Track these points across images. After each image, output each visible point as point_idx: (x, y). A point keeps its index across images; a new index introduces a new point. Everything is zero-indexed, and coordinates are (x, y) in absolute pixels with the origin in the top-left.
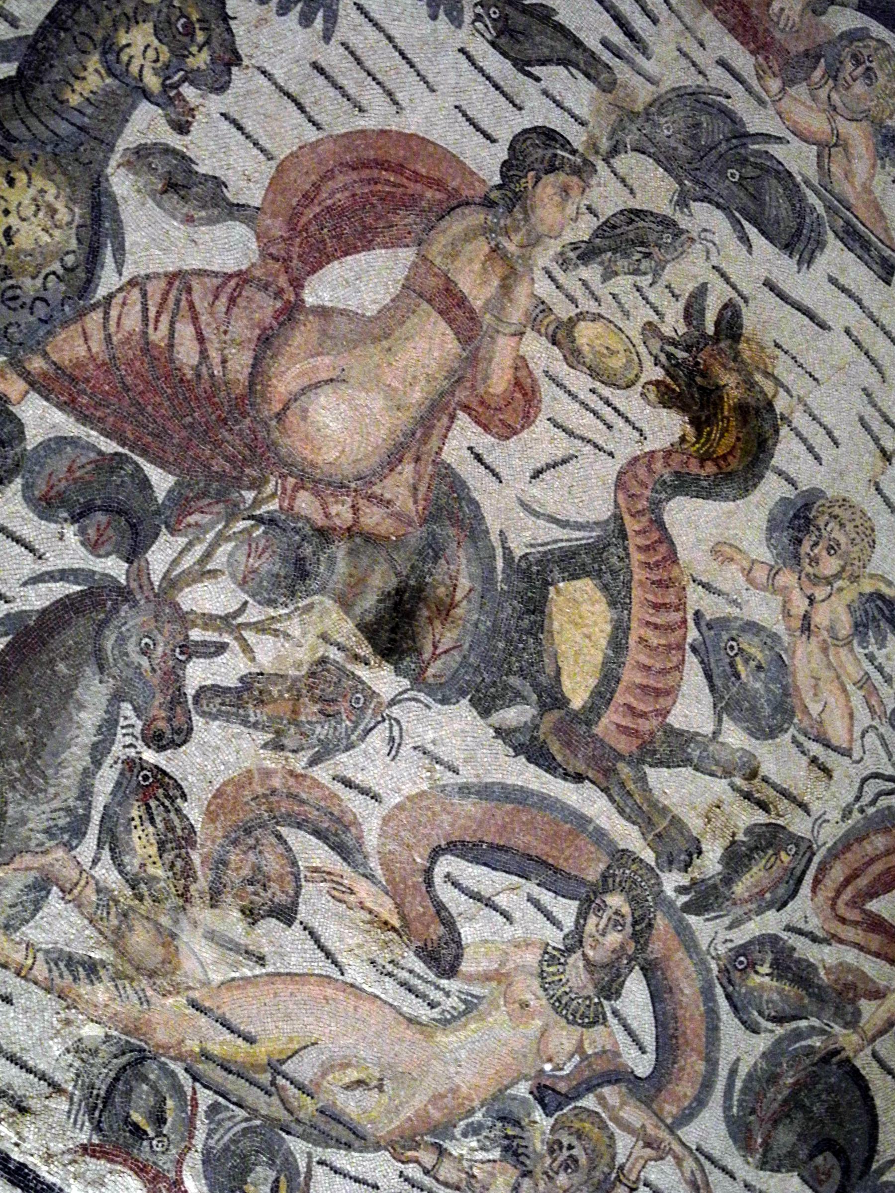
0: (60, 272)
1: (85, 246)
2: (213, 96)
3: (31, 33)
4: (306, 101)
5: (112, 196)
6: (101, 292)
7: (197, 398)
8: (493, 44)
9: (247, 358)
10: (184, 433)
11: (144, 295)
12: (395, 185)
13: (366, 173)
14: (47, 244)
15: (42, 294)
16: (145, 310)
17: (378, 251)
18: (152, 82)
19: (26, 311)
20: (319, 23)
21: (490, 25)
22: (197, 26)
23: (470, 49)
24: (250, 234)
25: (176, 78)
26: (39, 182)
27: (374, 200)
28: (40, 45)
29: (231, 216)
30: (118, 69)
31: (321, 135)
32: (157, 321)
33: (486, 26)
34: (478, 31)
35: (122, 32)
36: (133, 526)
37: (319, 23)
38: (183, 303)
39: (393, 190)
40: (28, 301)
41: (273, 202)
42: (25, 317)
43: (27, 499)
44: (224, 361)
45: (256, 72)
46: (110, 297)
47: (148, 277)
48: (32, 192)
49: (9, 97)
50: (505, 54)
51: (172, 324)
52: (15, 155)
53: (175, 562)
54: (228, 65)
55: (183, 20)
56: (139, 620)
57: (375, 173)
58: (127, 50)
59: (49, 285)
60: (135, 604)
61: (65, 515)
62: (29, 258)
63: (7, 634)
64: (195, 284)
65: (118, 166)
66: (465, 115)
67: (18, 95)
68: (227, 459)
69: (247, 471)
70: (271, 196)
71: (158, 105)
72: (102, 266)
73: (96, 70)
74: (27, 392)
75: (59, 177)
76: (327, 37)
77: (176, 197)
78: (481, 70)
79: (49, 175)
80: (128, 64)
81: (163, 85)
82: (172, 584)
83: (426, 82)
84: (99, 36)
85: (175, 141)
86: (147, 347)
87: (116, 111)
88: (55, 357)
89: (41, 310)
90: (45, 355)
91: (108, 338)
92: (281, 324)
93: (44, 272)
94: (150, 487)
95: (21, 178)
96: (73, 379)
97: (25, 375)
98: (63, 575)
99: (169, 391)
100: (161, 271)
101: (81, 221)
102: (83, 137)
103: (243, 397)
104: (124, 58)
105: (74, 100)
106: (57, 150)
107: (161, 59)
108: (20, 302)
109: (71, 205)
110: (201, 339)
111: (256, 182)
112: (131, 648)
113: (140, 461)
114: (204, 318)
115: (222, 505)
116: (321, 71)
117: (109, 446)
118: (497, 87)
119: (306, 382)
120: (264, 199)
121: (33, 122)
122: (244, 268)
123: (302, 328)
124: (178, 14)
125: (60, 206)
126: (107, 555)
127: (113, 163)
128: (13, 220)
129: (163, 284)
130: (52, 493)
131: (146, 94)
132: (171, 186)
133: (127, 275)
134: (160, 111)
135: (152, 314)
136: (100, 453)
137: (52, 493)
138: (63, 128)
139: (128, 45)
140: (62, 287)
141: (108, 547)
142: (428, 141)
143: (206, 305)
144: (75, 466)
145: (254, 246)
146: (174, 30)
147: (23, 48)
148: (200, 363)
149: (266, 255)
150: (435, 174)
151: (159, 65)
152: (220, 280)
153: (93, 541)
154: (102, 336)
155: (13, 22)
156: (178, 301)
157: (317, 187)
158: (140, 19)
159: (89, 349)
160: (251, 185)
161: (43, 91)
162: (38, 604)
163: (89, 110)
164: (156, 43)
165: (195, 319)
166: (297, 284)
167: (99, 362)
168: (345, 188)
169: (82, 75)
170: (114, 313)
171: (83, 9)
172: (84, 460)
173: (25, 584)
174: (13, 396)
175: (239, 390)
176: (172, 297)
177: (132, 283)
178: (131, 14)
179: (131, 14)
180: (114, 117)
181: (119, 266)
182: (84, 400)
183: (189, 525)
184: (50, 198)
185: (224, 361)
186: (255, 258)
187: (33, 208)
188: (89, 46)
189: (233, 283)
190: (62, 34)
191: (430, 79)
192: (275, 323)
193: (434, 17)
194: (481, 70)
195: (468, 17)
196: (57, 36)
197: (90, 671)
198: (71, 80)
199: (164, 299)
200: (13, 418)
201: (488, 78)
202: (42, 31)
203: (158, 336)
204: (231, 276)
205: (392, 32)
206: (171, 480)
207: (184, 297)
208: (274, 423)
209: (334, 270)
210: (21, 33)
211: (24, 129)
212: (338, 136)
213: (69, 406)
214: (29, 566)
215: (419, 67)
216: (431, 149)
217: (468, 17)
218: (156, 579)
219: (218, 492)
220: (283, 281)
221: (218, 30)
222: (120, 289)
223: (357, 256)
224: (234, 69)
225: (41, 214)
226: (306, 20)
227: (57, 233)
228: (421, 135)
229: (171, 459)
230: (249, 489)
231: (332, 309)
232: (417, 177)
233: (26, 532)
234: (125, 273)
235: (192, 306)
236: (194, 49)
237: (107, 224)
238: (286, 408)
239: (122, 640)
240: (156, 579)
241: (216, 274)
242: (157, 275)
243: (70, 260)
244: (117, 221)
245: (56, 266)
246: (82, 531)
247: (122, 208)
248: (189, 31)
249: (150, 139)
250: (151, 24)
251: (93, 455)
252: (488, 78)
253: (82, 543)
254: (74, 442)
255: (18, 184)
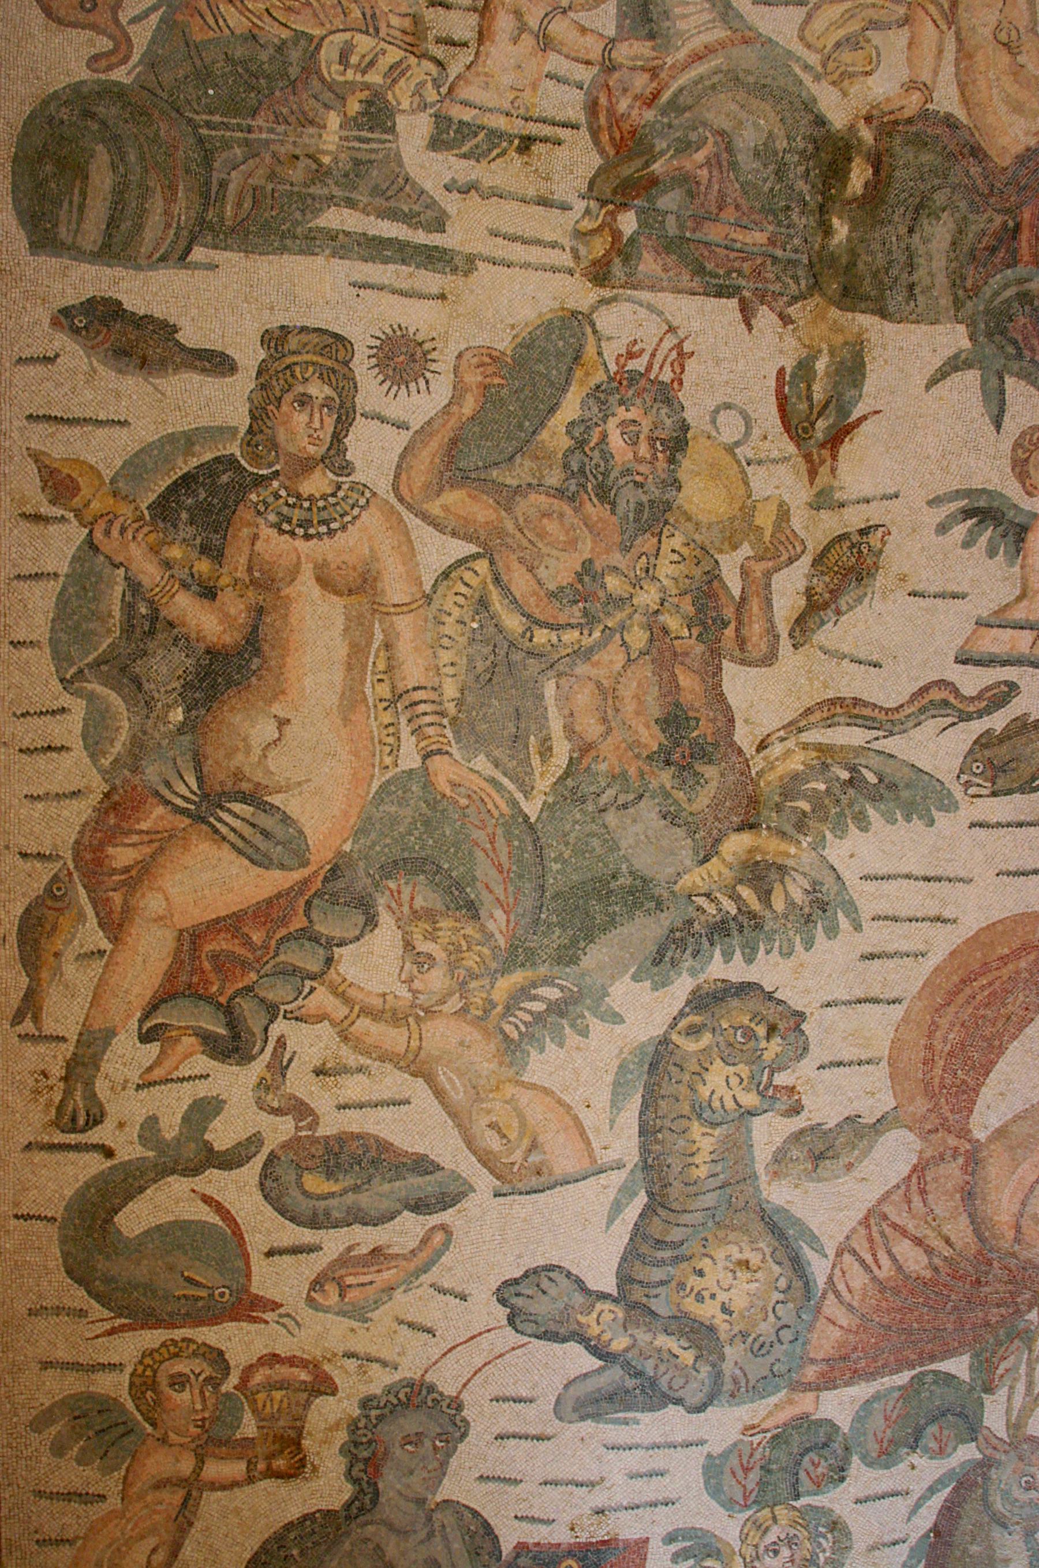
0: (781, 1297)
1: (787, 1262)
2: (802, 1062)
3: (637, 1159)
4: (875, 992)
5: (780, 1210)
6: (821, 1281)
7: (945, 1286)
8: (994, 794)
9: (964, 1220)
10: (952, 1318)
11: (854, 1252)
12: (990, 984)
13: (960, 999)
14: (758, 1289)
15: (780, 1324)
16: (862, 1262)
17: (1011, 1047)
18: (749, 1099)
19: (777, 1345)
20: (844, 922)
21: (981, 782)
22: (753, 1025)
23: (980, 817)
24: (904, 1132)
25: (765, 1078)
26: (720, 1254)
27: (982, 1012)
28: (650, 1161)
29: (879, 1133)
30: (717, 1117)
31: (905, 1004)
32: (876, 1261)
33: (979, 785)
34: (973, 796)
35: (700, 1087)
36: (959, 1415)
37: (844, 922)
38: (888, 1230)
39: (991, 989)
40: (774, 1338)
41: (903, 1091)
42: (779, 1350)
43: (870, 1465)
44: (947, 1241)
45: (822, 1011)
46: (830, 1279)
47: (848, 1238)
48: (720, 1265)
49: (655, 1218)
50: (1009, 792)
51: (889, 1253)
52: (688, 1253)
53: (1008, 1411)
54: (797, 1028)
55: (739, 1033)
56: (1009, 1471)
57: (968, 991)
58: (714, 1096)
59: (780, 1314)
60: (999, 1463)
61: (906, 1450)
62: (752, 1310)
63: (919, 1561)
64: (887, 1209)
65: (769, 1184)
66: (1009, 873)
67: (660, 1210)
68: (998, 1306)
69: (1019, 1300)
70: (898, 1088)
71: (766, 1111)
72: (809, 1264)
73: (703, 1134)
74: (818, 1397)
75: (732, 1236)
76: (858, 927)
77: (827, 1162)
78: (999, 825)
79: (724, 1242)
80: (723, 1107)
81: (759, 1093)
82: (1016, 1426)
83: (961, 880)
84: (686, 1109)
85: (798, 1123)
86: (882, 1286)
87: (740, 1148)
88: (820, 1356)
89: (787, 1335)
90: (813, 1361)
91: (850, 1307)
92: (972, 1174)
93: (770, 1309)
94: (954, 1377)
95: (705, 1264)
96: (844, 1358)
97: (808, 1387)
98: (932, 1490)
99: (921, 1300)
100: (854, 1224)
101: (771, 1249)
102: (728, 1190)
103: (980, 1252)
104: (716, 1104)
105: (702, 1172)
106: (717, 1219)
107: (743, 1076)
108: (767, 1345)
109: (755, 1246)
110: (918, 1242)
111: (880, 1090)
112: (1017, 1493)
113: (933, 1367)
114: (910, 1227)
115: (1016, 1341)
116: (872, 957)
117: (904, 1377)
118: (1020, 825)
119: (1021, 1196)
120: (895, 1097)
121: (687, 1218)
122: (915, 1161)
123: (991, 1160)
124: (732, 1031)
125: (747, 1255)
126: (955, 1449)
127: (763, 1186)
128: (723, 1296)
129: (863, 1231)
130: (885, 1445)
131: (751, 1113)
132: (818, 1158)
133: (831, 1252)
134: (770, 1114)
135: (868, 1258)
136: (900, 1388)
137: (885, 1445)
138: (709, 1200)
139: (713, 1092)
140: (791, 1305)
141: (951, 1445)
142: (994, 924)
143: (905, 1214)
144: (888, 1413)
145: (911, 1137)
146: (738, 1046)
147: (639, 1175)
148: (930, 1259)
149: (925, 1135)
150: (1016, 944)
151: (745, 1083)
152: (903, 1187)
153: (937, 1449)
154: (844, 1310)
155: (619, 1166)
156: (882, 1234)
157: (930, 1047)
158: (707, 1065)
159: (841, 1327)
160: (877, 1096)
161: (676, 1190)
162: (928, 1524)
163: (719, 1168)
164: (732, 1069)
165: (904, 1233)
166: (964, 1133)
167: (854, 1329)
168: (953, 1025)
169: (694, 1149)
170: (841, 1287)
171: (661, 1102)
172: (891, 1403)
173: (909, 1519)
174: (810, 1409)
175: (973, 1249)
176: (876, 1235)
177: (839, 1254)
178: (698, 1069)
179: (698, 1069)
180: (741, 1152)
181: (821, 1252)
182: (863, 1363)
183: (1002, 1376)
184: (737, 1256)
185: (947, 1241)
186: (918, 1145)
187: (730, 1274)
188: (684, 1122)
189: (914, 1180)
190: (660, 1136)
191: (962, 874)
192: (967, 1178)
193: (931, 823)
194: (999, 825)
195: (958, 792)
196: (657, 1141)
197: (997, 1532)
198: (690, 1160)
199: (871, 1240)
200: (820, 1423)
201: (1009, 825)
202: (644, 1150)
203: (886, 1270)
204: (909, 1177)
205: (905, 870)
206: (966, 1359)
207: (884, 1226)
208: (1017, 1247)
209: (987, 1094)
210: (630, 1166)
211: (683, 1229)
212: (919, 993)
213: (856, 1376)
214: (902, 1505)
215: (945, 874)
216: (1000, 928)
217: (958, 792)
218: (1003, 1434)
219: (1008, 1335)
220: (952, 1141)
221: (772, 1011)
222: (834, 1266)
223: (997, 1067)
224: (804, 1026)
225: (739, 1274)
226: (832, 931)
227: (759, 1275)
228: (984, 925)
229: (956, 1344)
230: (1029, 1311)
231: (1006, 1125)
232: (1004, 960)
233: (884, 1487)
234: (828, 1253)
235: (895, 1226)
236: (763, 1044)
237: (791, 1232)
238: (1018, 1229)
239: (1006, 1494)
240: (1003, 1434)
241: (897, 1186)
242: (854, 1230)
243: (782, 1283)
244: (798, 1222)
245: (777, 1296)
246: (926, 1450)
247: (793, 1210)
248: (750, 1035)
249: (778, 1141)
250: (719, 1060)
251: (896, 1394)
252: (1009, 825)
253: (931, 1458)
254: (876, 1397)
255: (706, 1270)
